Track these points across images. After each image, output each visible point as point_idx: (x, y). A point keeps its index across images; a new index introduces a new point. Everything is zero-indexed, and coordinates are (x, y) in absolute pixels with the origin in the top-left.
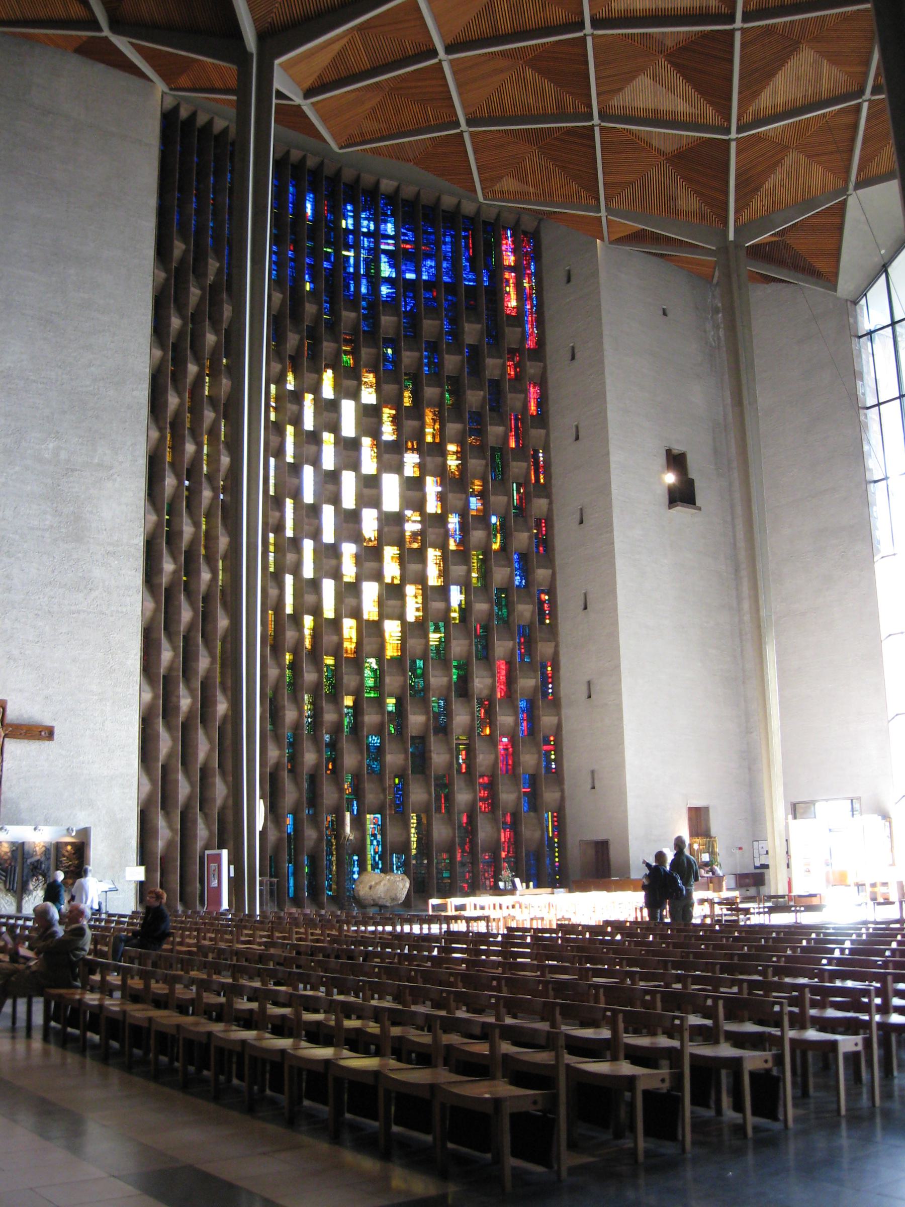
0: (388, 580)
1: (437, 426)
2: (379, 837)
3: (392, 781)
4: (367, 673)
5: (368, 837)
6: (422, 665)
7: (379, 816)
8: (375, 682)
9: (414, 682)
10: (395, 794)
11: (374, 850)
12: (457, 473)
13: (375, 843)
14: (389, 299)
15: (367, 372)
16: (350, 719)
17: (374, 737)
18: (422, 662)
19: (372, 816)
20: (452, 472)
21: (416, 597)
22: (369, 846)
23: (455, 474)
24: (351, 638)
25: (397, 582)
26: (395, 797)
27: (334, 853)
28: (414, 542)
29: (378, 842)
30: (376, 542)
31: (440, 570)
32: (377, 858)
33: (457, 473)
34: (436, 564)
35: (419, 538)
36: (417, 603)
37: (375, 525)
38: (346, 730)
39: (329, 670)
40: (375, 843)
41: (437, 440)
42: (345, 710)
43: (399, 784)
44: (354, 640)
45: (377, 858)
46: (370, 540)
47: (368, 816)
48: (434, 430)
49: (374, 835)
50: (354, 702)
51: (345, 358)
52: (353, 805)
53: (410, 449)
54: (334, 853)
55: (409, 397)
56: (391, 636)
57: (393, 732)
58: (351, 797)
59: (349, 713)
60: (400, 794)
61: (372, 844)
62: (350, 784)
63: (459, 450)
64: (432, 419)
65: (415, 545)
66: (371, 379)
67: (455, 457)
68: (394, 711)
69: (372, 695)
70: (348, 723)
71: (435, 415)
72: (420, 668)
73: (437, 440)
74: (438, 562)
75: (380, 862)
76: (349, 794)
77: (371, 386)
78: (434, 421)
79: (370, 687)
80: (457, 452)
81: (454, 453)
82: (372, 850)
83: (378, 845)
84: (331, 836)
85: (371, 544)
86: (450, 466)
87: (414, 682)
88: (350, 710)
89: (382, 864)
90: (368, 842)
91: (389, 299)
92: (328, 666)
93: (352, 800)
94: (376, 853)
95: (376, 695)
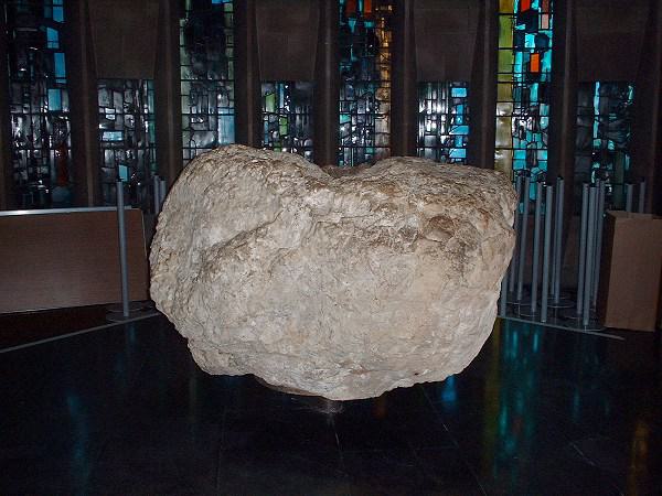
2: (545, 22)
5: (504, 21)
11: (527, 65)
13: (530, 41)
22: (505, 56)
27: (385, 75)
29: (541, 38)
32: (534, 95)
40: (530, 41)
45: (534, 95)
49: (528, 17)
54: (385, 75)
61: (518, 45)
75: (543, 108)
82: (519, 69)
83: (540, 50)
84: (371, 18)
89: (550, 115)
90: (506, 41)
94: (532, 77)
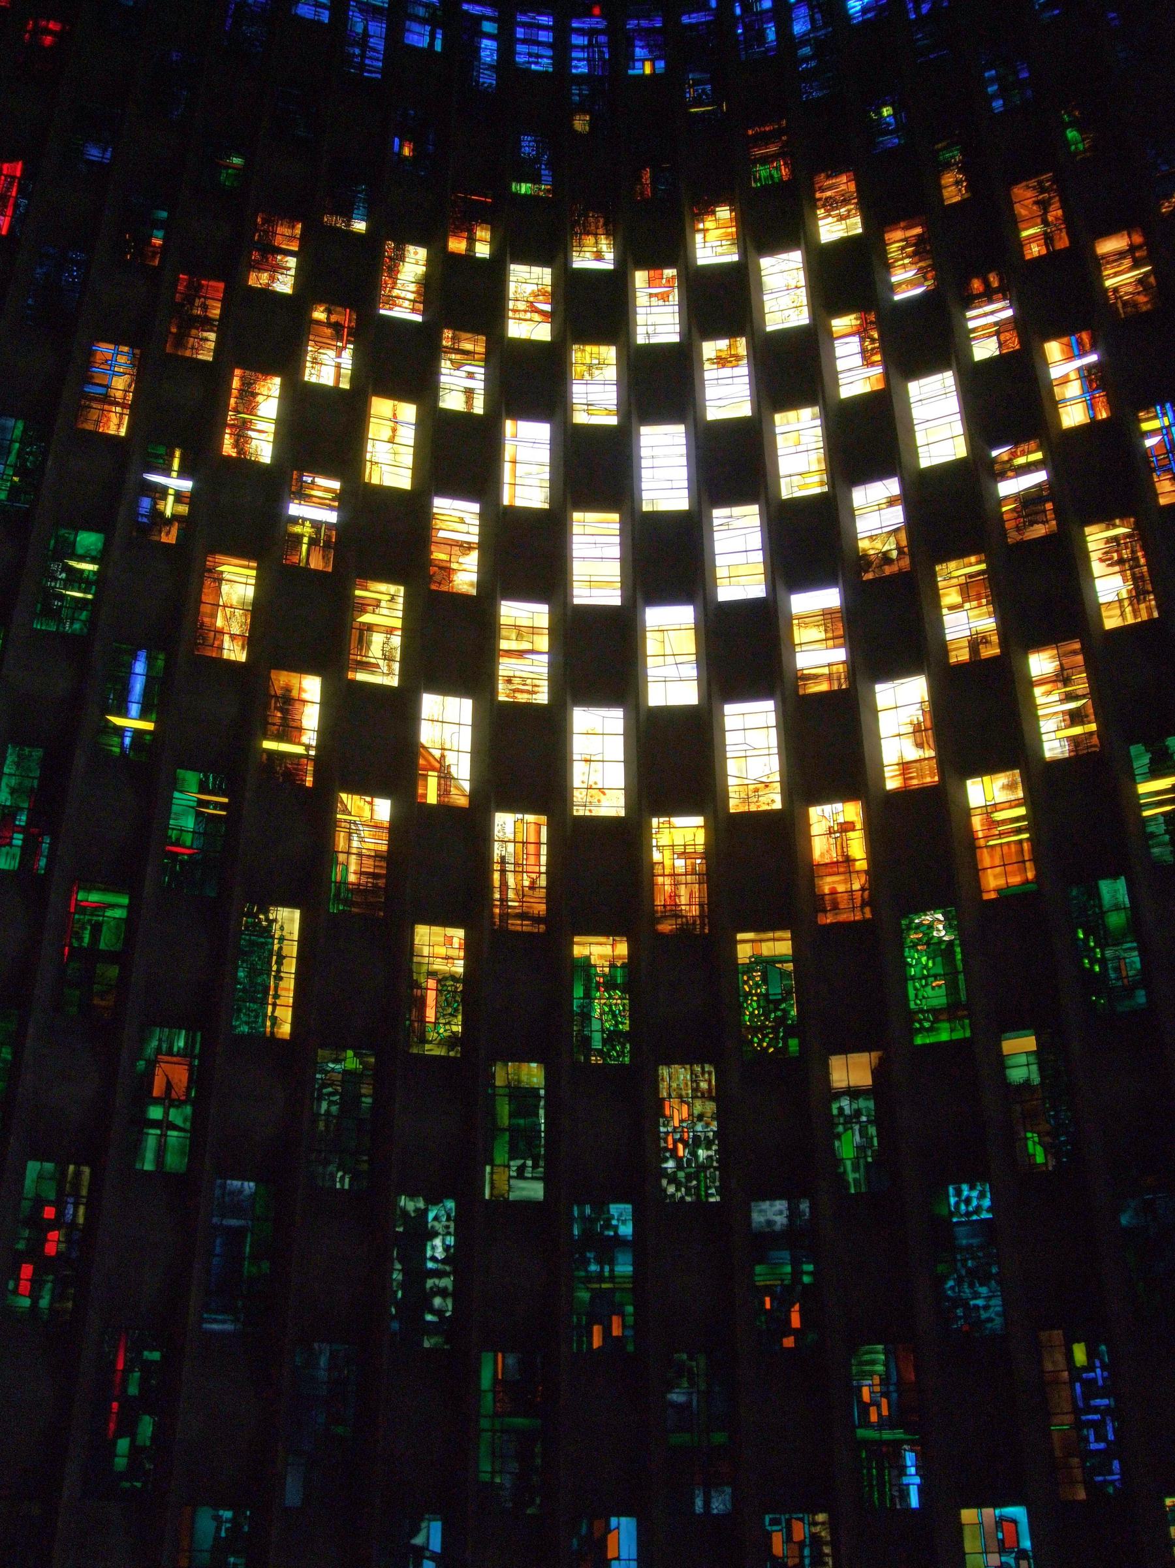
0: (960, 655)
1: (1055, 213)
3: (1060, 1357)
4: (918, 961)
6: (1123, 897)
7: (1018, 1512)
8: (952, 988)
9: (1103, 962)
10: (1077, 1411)
12: (1142, 299)
14: (869, 16)
15: (828, 177)
16: (863, 1133)
17: (965, 1187)
18: (1121, 885)
19: (990, 1514)
20: (1125, 304)
21: (1066, 681)
23: (1135, 305)
24: (848, 860)
25: (989, 652)
26: (1079, 1425)
28: (1032, 524)
30: (906, 562)
31: (1135, 579)
33: (1142, 299)
34: (1121, 561)
35: (1049, 506)
36: (1070, 697)
37: (896, 516)
38: (851, 1176)
39: (773, 976)
41: (1062, 242)
42: (845, 1103)
43: (1090, 1367)
44: (862, 865)
46: (885, 558)
47: (968, 1515)
48: (1045, 222)
50: (877, 1073)
51: (763, 171)
52: (902, 1471)
53: (979, 296)
55: (957, 183)
56: (991, 824)
57: (1040, 1159)
58: (887, 1435)
59: (858, 1113)
60: (1107, 1411)
62: (885, 1381)
63: (1138, 239)
64: (1036, 203)
65: (1039, 531)
66: (843, 187)
67: (1127, 263)
68: (1036, 1079)
69: (944, 1037)
70: (860, 1149)
71: (1042, 190)
72: (1117, 908)
73: (1062, 242)
74: (1126, 554)
76: (882, 1424)
77: (846, 202)
78: (1044, 205)
79: (933, 1011)
80: (1132, 249)
81: (1121, 255)
85: (888, 570)
86: (1116, 290)
87: (1103, 962)
88: (862, 1103)
91: (869, 16)
92: (766, 964)
93: (897, 1445)
95: (959, 1035)
